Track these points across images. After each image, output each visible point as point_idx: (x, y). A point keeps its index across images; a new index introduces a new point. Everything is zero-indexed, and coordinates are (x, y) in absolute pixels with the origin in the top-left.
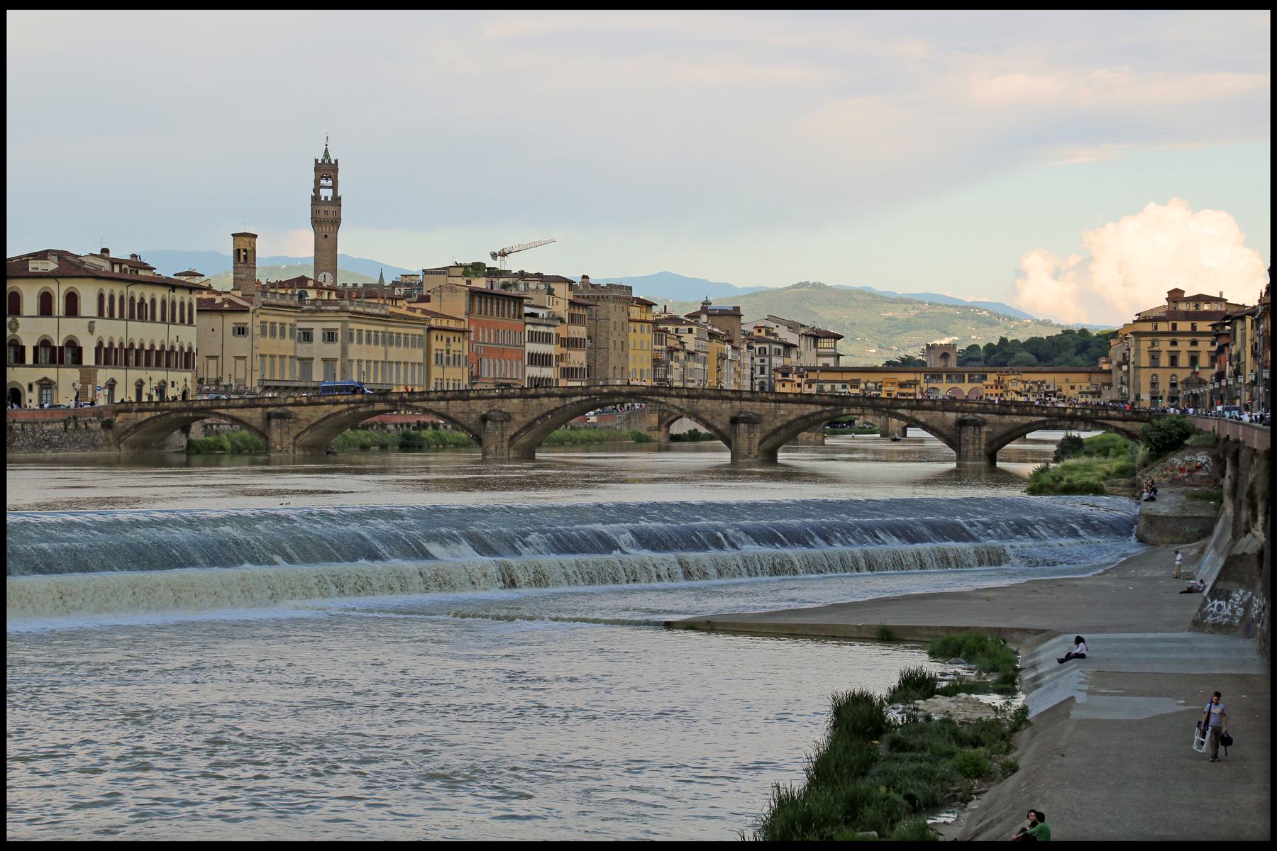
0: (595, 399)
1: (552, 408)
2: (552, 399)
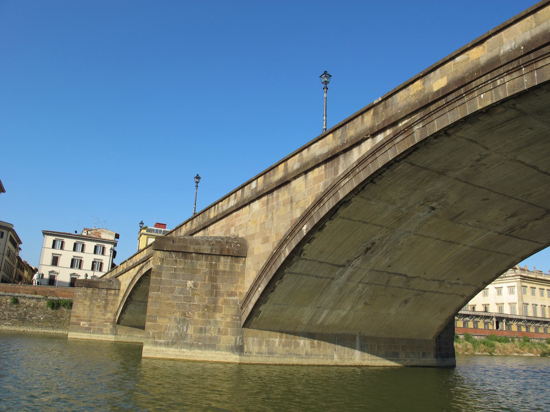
0: (410, 127)
2: (311, 175)
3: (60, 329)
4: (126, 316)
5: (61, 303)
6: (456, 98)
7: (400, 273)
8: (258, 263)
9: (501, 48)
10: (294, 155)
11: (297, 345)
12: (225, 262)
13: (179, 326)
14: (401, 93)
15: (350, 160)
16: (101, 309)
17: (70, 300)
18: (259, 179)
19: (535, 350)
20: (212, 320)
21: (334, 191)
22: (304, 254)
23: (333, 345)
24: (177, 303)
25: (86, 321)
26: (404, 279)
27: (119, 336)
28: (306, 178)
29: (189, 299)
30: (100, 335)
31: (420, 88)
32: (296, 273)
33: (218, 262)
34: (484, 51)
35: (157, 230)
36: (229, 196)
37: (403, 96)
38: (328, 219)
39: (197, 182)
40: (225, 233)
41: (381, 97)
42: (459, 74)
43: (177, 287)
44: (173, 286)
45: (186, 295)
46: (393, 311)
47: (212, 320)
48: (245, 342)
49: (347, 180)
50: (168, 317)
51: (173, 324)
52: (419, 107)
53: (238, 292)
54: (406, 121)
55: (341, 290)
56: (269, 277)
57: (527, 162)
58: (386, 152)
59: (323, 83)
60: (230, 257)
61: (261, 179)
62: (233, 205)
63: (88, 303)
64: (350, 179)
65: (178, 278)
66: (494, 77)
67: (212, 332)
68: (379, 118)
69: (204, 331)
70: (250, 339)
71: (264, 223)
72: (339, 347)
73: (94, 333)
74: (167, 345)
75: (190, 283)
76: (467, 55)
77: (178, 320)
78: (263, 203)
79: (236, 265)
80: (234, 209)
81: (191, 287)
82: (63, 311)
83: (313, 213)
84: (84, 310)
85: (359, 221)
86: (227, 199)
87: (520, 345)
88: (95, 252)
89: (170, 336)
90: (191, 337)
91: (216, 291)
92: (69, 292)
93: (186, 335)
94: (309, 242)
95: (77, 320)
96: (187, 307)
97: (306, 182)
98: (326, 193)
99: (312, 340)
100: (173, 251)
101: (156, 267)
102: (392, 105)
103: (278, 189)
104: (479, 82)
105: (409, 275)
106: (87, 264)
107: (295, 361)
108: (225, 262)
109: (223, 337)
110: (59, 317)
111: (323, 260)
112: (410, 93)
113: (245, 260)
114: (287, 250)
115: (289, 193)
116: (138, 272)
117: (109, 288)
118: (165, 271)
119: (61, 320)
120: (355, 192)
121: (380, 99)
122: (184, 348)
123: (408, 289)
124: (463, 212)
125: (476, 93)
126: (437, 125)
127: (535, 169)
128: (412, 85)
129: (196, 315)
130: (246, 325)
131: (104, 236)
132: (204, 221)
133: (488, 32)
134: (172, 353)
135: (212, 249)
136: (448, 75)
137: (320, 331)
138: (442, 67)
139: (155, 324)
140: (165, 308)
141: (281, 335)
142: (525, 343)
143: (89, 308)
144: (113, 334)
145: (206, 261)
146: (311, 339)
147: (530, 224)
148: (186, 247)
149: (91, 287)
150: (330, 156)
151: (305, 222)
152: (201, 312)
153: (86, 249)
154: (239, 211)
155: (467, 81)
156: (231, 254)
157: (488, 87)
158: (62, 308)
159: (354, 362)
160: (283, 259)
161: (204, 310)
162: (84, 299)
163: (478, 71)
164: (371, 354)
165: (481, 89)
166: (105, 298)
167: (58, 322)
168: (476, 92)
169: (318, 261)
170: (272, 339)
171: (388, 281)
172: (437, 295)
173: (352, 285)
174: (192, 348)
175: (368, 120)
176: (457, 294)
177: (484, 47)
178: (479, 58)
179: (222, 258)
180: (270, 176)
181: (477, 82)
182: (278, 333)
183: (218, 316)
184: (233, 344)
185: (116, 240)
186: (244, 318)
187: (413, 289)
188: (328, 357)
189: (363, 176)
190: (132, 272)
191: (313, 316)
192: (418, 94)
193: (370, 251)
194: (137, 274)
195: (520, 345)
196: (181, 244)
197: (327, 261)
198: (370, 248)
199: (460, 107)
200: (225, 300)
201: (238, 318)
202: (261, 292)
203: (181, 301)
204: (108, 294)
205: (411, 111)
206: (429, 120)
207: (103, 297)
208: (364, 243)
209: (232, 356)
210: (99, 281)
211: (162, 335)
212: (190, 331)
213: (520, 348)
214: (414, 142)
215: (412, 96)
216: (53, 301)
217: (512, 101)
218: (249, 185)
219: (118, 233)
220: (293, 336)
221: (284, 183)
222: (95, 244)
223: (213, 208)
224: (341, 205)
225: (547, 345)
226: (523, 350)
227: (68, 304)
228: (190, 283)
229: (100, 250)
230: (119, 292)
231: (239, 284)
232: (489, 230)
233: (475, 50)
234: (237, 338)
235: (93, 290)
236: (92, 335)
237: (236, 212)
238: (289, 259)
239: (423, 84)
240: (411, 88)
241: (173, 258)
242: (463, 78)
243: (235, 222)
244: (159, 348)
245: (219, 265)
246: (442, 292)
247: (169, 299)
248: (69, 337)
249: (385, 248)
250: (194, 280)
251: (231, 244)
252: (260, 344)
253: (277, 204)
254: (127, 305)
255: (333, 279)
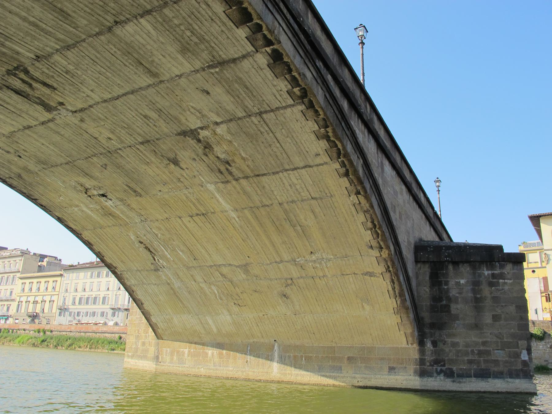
72: (252, 358)
146: (219, 350)
164: (295, 367)
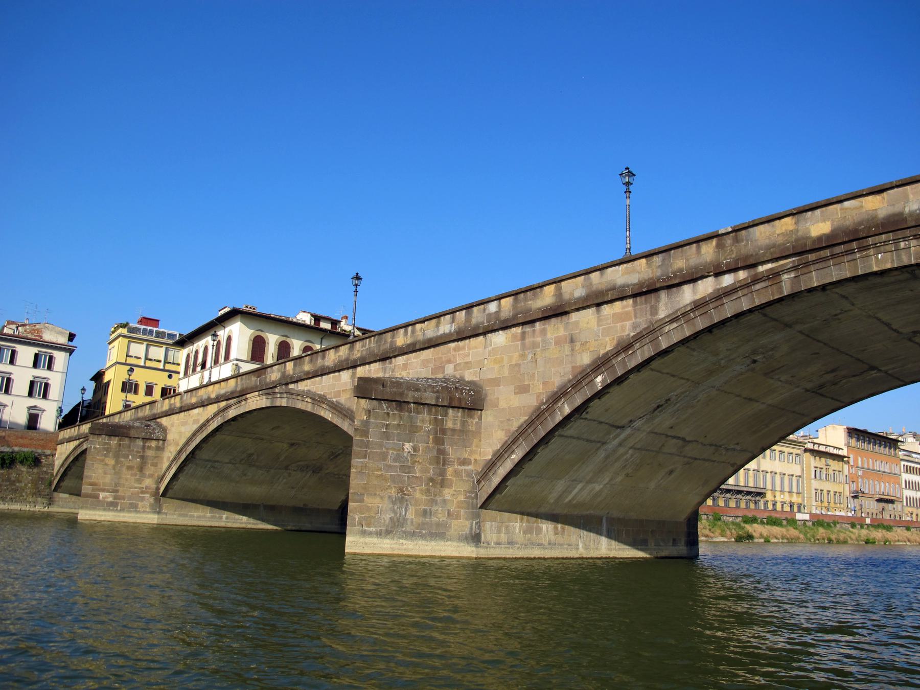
0: (775, 275)
1: (609, 346)
2: (606, 309)
3: (15, 502)
4: (177, 486)
5: (18, 456)
6: (845, 252)
7: (680, 435)
8: (509, 420)
9: (906, 205)
10: (575, 276)
11: (539, 530)
12: (454, 417)
13: (396, 508)
14: (761, 227)
15: (678, 299)
16: (133, 472)
17: (32, 452)
18: (503, 301)
19: (728, 533)
20: (438, 499)
21: (651, 337)
22: (587, 413)
23: (577, 530)
24: (391, 475)
25: (108, 491)
26: (680, 442)
27: (164, 516)
28: (598, 312)
29: (408, 469)
30: (133, 515)
31: (791, 228)
32: (566, 437)
33: (446, 416)
34: (883, 203)
35: (145, 331)
36: (438, 316)
37: (765, 232)
38: (636, 371)
39: (356, 285)
40: (434, 371)
41: (731, 227)
42: (848, 223)
43: (391, 452)
44: (385, 451)
45: (404, 462)
46: (652, 485)
47: (438, 499)
48: (482, 528)
49: (675, 325)
50: (379, 495)
51: (386, 505)
52: (792, 252)
53: (472, 458)
54: (769, 266)
55: (607, 457)
56: (532, 440)
57: (884, 320)
58: (738, 300)
59: (624, 184)
60: (461, 410)
61: (507, 303)
62: (447, 331)
63: (111, 462)
64: (679, 324)
65: (392, 438)
66: (897, 238)
67: (440, 516)
68: (727, 254)
69: (428, 514)
70: (488, 525)
71: (518, 365)
73: (122, 510)
74: (379, 534)
75: (408, 446)
76: (860, 202)
77: (394, 499)
78: (514, 337)
79: (470, 420)
80: (454, 338)
81: (410, 452)
82: (20, 470)
83: (614, 361)
84: (105, 473)
85: (668, 374)
86: (434, 321)
87: (709, 526)
88: (35, 365)
89: (383, 521)
90: (412, 522)
91: (444, 458)
92: (31, 439)
93: (405, 520)
94: (599, 398)
95: (93, 490)
96: (404, 480)
97: (599, 317)
98: (639, 337)
99: (555, 523)
100: (384, 400)
101: (360, 423)
102: (747, 241)
103: (544, 320)
104: (877, 240)
105: (687, 439)
106: (20, 386)
107: (536, 553)
108: (454, 417)
109: (454, 522)
110: (14, 481)
111: (603, 420)
112: (775, 231)
113: (481, 415)
114: (566, 406)
115: (566, 328)
116: (216, 415)
117: (147, 437)
118: (373, 428)
119: (18, 487)
120: (684, 342)
121: (730, 230)
122: (402, 538)
123: (679, 456)
124: (783, 366)
125: (872, 252)
126: (815, 279)
127: (887, 326)
128: (778, 221)
129: (418, 491)
130: (484, 506)
131: (48, 336)
132: (382, 348)
133: (892, 183)
134: (386, 546)
135: (437, 398)
136: (832, 220)
137: (565, 512)
138: (824, 209)
139: (362, 506)
140: (375, 482)
141: (522, 518)
142: (716, 522)
143: (114, 469)
144: (155, 513)
145: (429, 414)
147: (844, 381)
148: (402, 394)
149: (116, 436)
150: (646, 289)
151: (600, 371)
152: (424, 487)
153: (19, 360)
154: (463, 342)
155: (862, 235)
156: (463, 406)
157: (888, 248)
158: (19, 466)
159: (600, 553)
160: (559, 418)
161: (428, 484)
162: (105, 455)
163: (877, 226)
164: (619, 542)
165: (878, 248)
166: (141, 454)
167: (12, 489)
168: (872, 250)
169: (598, 421)
170: (511, 524)
171: (663, 445)
172: (707, 464)
173: (622, 450)
174: (414, 538)
175: (708, 251)
176: (729, 463)
177: (883, 198)
178: (876, 210)
179: (450, 411)
180: (526, 300)
181: (875, 239)
182: (519, 515)
183: (447, 493)
184: (468, 532)
185: (70, 343)
186: (483, 496)
187: (685, 457)
188: (572, 547)
189: (701, 324)
190: (198, 413)
191: (564, 492)
192: (787, 235)
193: (660, 409)
194: (212, 418)
195: (709, 526)
196: (394, 390)
197: (607, 421)
198: (662, 406)
199: (849, 263)
200: (456, 471)
201: (473, 495)
202: (516, 461)
203: (396, 472)
204: (146, 447)
205: (779, 256)
206: (805, 270)
207: (138, 452)
208: (658, 399)
209: (466, 548)
210: (130, 426)
211: (373, 521)
212: (411, 515)
213: (710, 530)
214: (782, 292)
215: (778, 235)
216: (2, 454)
217: (915, 268)
218: (482, 307)
219: (73, 332)
220: (534, 519)
221: (558, 312)
222: (35, 350)
223: (402, 331)
224: (659, 356)
225: (742, 524)
226: (713, 533)
227: (31, 459)
228: (408, 446)
229: (43, 360)
230: (164, 444)
231: (474, 448)
232: (798, 387)
233: (870, 198)
234: (472, 523)
235: (120, 440)
236: (118, 514)
237: (456, 343)
238: (567, 419)
239: (795, 223)
240: (777, 224)
241: (384, 410)
242: (856, 231)
243: (454, 357)
244: (368, 540)
245: (446, 421)
246: (714, 460)
247: (380, 469)
248: (79, 517)
249: (678, 405)
250: (413, 442)
251: (461, 391)
252: (499, 531)
253: (544, 341)
254: (185, 465)
255: (604, 443)
